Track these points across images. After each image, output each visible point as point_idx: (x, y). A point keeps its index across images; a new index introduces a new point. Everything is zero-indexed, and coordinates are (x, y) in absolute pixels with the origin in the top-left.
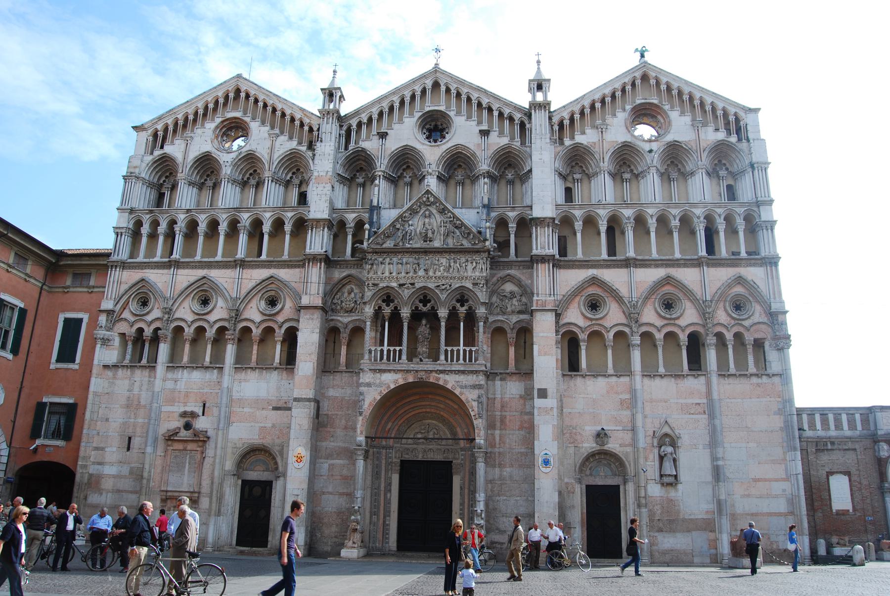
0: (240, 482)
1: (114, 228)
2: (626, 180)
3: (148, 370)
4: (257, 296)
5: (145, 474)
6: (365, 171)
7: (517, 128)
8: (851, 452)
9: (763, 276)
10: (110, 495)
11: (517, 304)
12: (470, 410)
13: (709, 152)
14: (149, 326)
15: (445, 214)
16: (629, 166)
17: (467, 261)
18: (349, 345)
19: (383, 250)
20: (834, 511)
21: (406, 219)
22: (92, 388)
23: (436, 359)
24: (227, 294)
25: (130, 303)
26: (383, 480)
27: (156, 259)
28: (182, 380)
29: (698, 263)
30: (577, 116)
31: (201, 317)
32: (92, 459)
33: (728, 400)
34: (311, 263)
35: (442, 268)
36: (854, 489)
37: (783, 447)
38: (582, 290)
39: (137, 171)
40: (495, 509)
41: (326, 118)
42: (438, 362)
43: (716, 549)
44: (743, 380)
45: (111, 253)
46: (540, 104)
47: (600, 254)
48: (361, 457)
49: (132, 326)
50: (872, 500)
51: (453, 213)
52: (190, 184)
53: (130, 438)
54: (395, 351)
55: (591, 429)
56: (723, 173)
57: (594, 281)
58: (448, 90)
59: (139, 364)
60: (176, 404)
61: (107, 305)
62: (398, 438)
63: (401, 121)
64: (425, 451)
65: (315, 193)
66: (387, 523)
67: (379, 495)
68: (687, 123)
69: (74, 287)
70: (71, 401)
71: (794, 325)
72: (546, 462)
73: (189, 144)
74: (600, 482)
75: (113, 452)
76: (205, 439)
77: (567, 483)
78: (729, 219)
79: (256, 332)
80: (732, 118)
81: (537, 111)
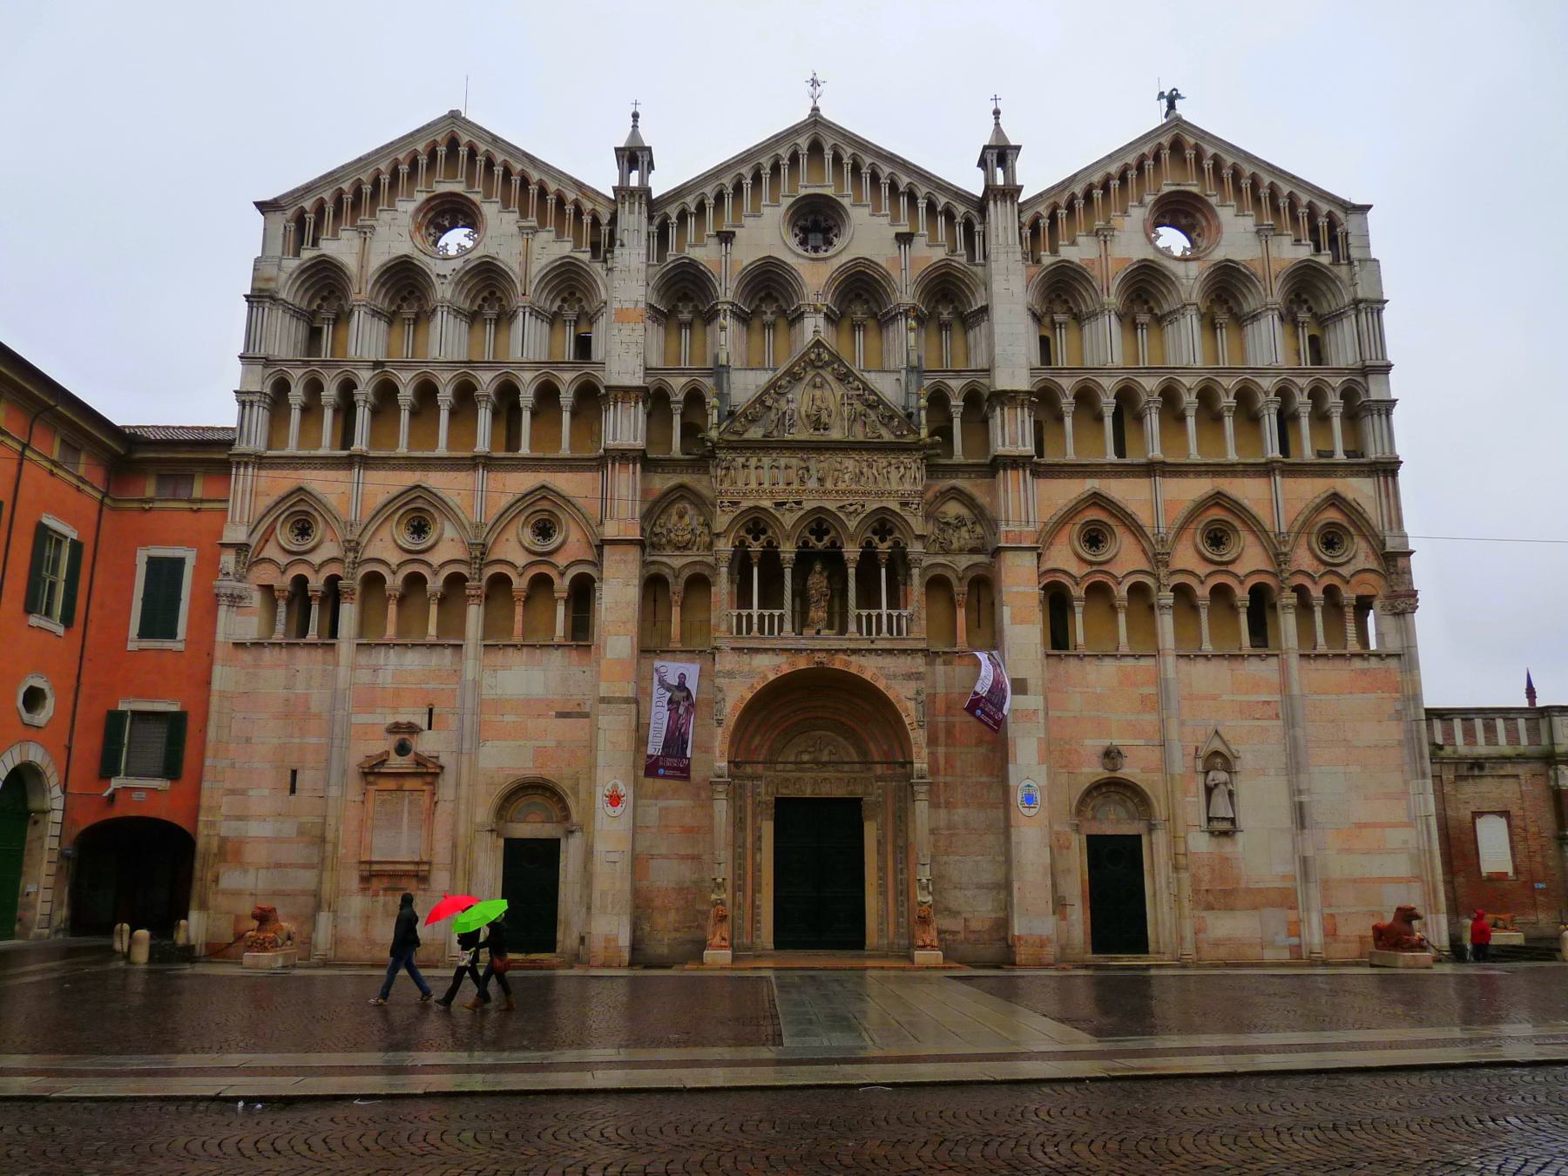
0: (501, 842)
1: (236, 392)
2: (1142, 325)
3: (320, 651)
4: (516, 520)
5: (330, 835)
6: (692, 300)
7: (960, 231)
8: (1513, 780)
9: (1371, 493)
10: (262, 873)
11: (967, 537)
12: (903, 715)
13: (1285, 280)
14: (317, 572)
15: (849, 383)
16: (1146, 302)
17: (890, 464)
18: (682, 607)
19: (744, 445)
20: (1484, 874)
21: (782, 391)
22: (216, 685)
23: (843, 630)
24: (461, 515)
25: (278, 531)
26: (749, 831)
27: (321, 452)
28: (387, 667)
29: (1266, 470)
30: (1062, 213)
31: (416, 557)
32: (224, 810)
33: (1315, 697)
34: (617, 464)
35: (847, 477)
36: (1516, 838)
37: (1402, 772)
38: (1076, 514)
39: (272, 285)
40: (941, 877)
41: (627, 203)
42: (847, 636)
43: (1299, 936)
44: (1339, 663)
45: (235, 440)
46: (1004, 190)
47: (1105, 455)
48: (723, 796)
49: (283, 573)
50: (1543, 857)
51: (863, 383)
52: (376, 313)
53: (294, 773)
54: (771, 616)
55: (1095, 744)
56: (1303, 316)
57: (1097, 500)
58: (837, 160)
59: (304, 641)
60: (379, 710)
61: (236, 533)
62: (770, 762)
63: (756, 213)
64: (816, 782)
65: (617, 339)
66: (757, 903)
67: (745, 859)
68: (1249, 229)
69: (161, 500)
70: (174, 708)
71: (1422, 572)
72: (1029, 799)
73: (368, 239)
74: (1108, 829)
75: (264, 795)
76: (438, 771)
77: (1058, 833)
78: (1317, 395)
79: (520, 583)
80: (1322, 222)
81: (999, 203)
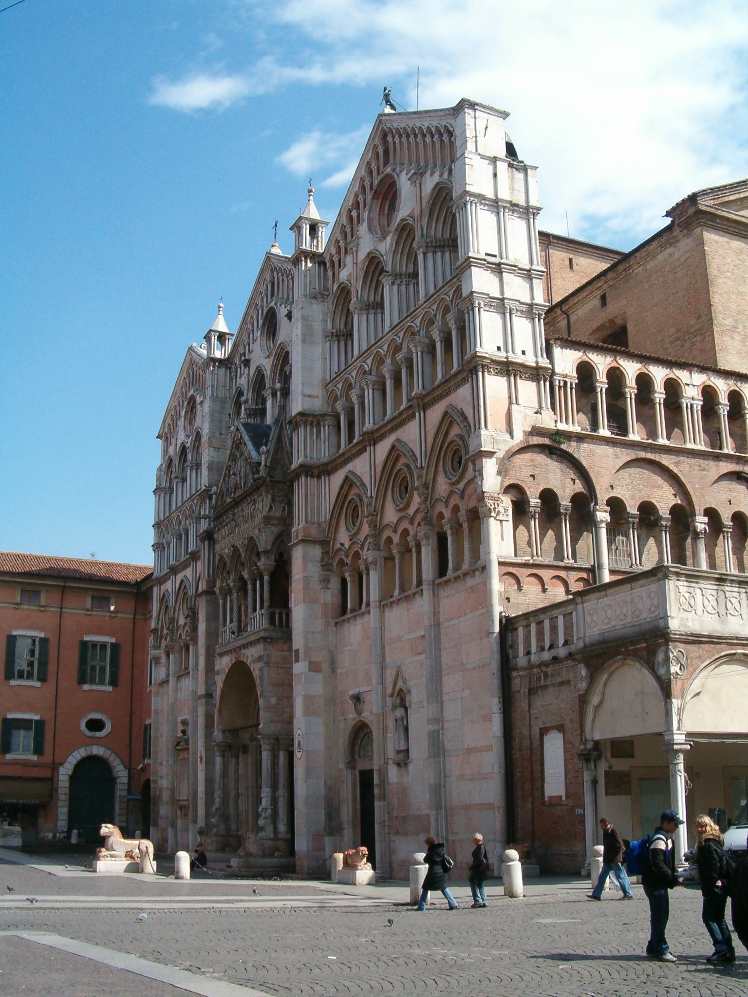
32: (159, 775)
33: (447, 624)
